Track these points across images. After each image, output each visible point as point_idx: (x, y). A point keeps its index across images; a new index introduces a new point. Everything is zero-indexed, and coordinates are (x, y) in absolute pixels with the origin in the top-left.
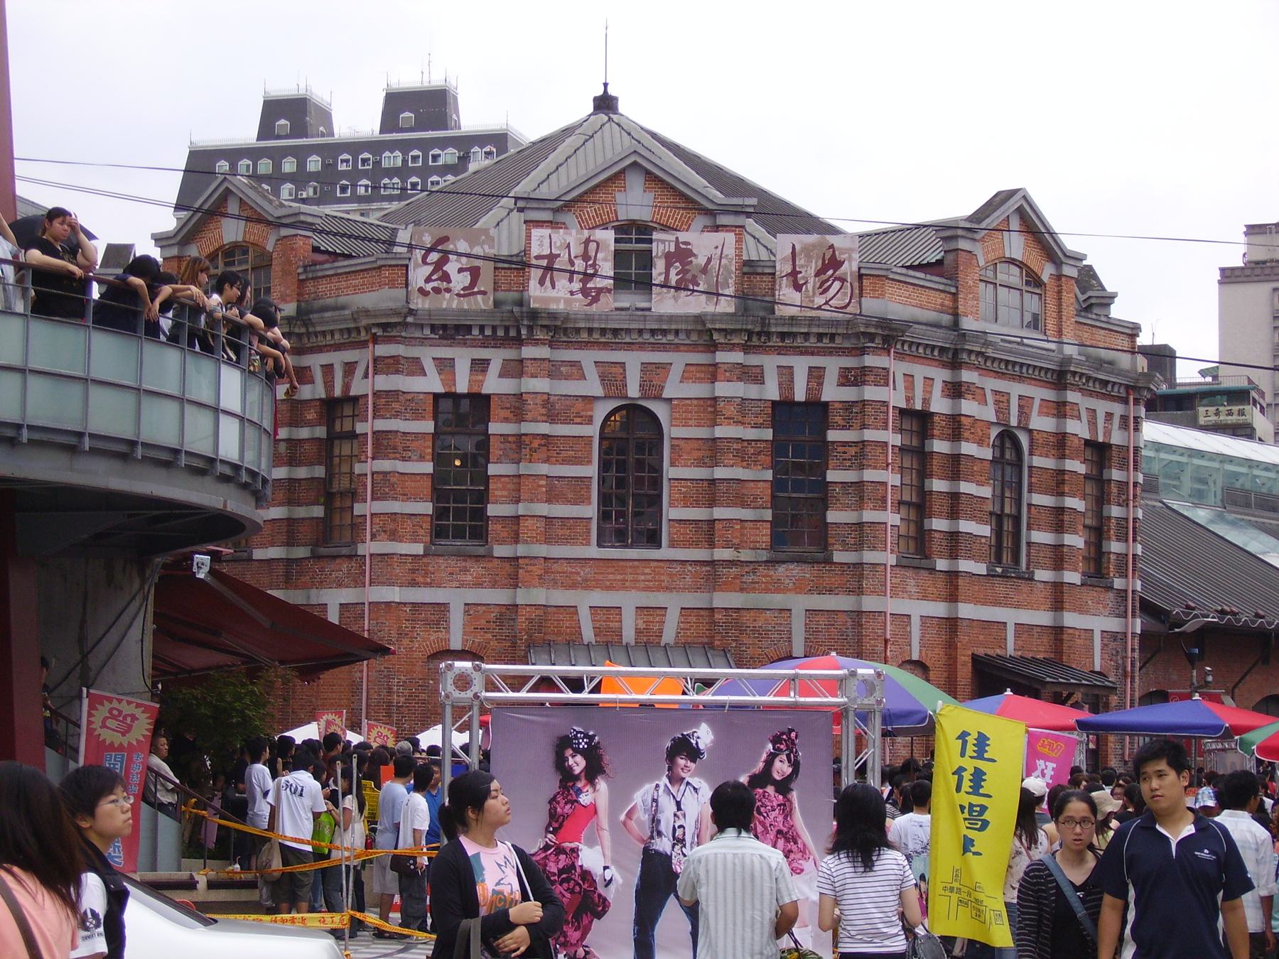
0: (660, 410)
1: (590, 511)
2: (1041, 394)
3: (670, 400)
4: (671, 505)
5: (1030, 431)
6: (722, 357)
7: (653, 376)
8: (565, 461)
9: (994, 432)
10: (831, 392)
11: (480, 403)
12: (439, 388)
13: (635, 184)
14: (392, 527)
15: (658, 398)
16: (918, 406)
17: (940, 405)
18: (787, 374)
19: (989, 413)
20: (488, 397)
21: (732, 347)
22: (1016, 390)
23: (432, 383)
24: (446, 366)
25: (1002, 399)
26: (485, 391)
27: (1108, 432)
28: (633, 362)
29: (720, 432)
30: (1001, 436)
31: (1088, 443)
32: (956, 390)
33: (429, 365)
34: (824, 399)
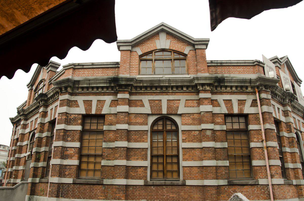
0: (177, 120)
1: (147, 163)
3: (180, 115)
4: (184, 160)
6: (202, 95)
8: (136, 141)
9: (295, 131)
10: (248, 109)
12: (84, 112)
13: (163, 36)
14: (62, 171)
15: (176, 114)
16: (278, 118)
17: (283, 119)
18: (228, 102)
21: (205, 91)
23: (81, 110)
24: (88, 103)
26: (103, 112)
29: (204, 126)
32: (286, 114)
33: (81, 103)
34: (246, 112)
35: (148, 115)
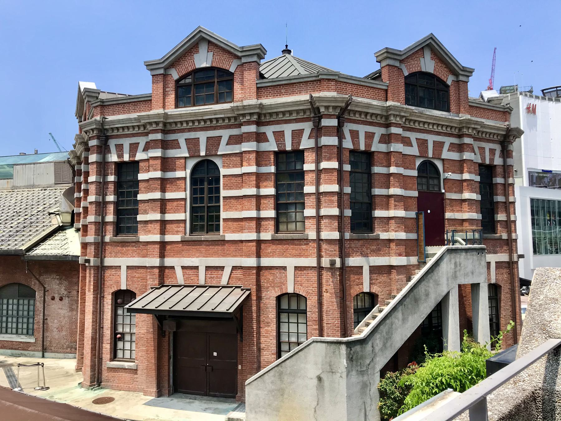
0: (218, 162)
2: (448, 141)
5: (443, 160)
7: (214, 142)
9: (418, 162)
11: (134, 165)
15: (217, 155)
18: (279, 135)
19: (414, 150)
20: (137, 162)
22: (431, 139)
25: (423, 144)
27: (492, 160)
28: (203, 136)
30: (423, 164)
31: (480, 165)
34: (301, 147)
35: (186, 158)
